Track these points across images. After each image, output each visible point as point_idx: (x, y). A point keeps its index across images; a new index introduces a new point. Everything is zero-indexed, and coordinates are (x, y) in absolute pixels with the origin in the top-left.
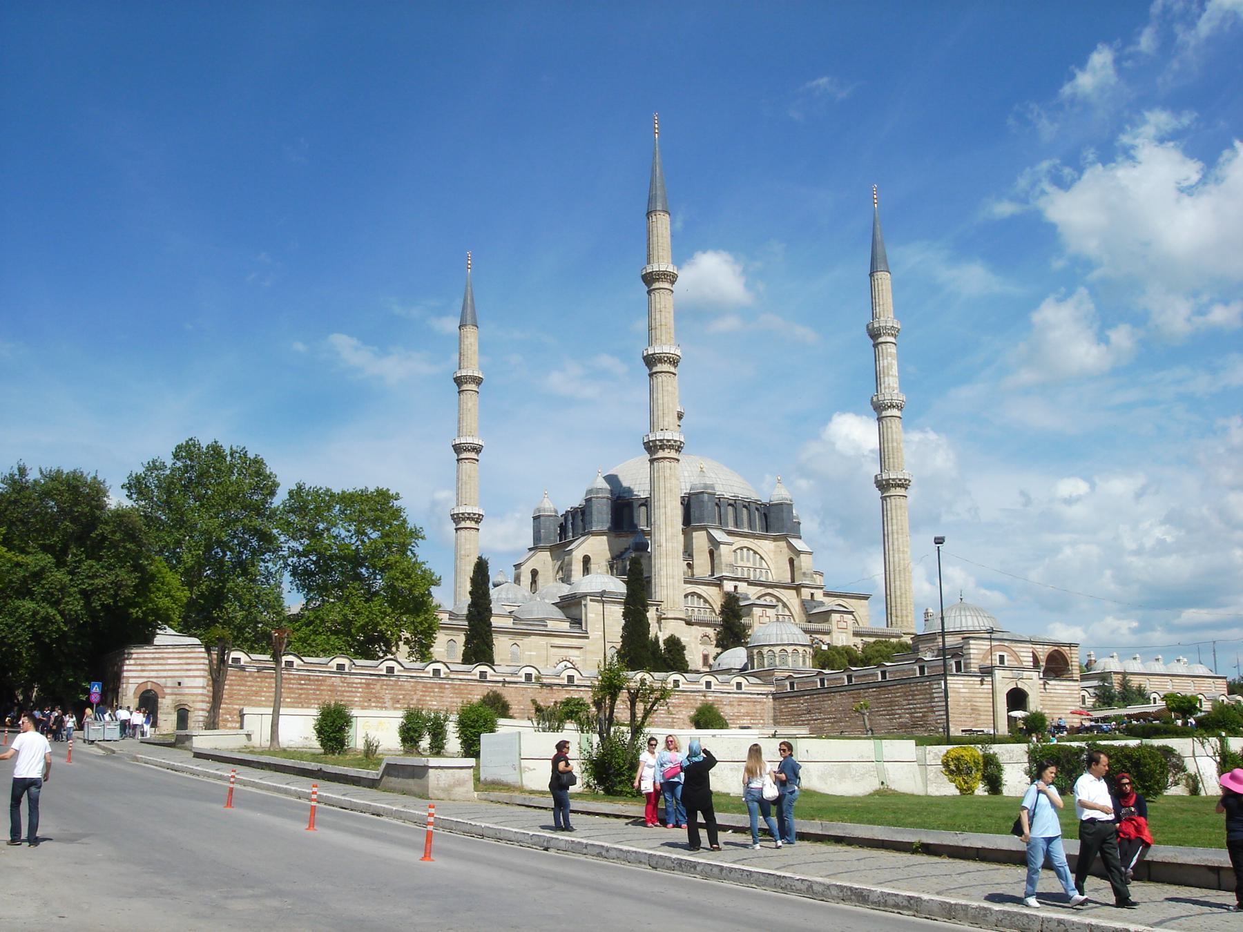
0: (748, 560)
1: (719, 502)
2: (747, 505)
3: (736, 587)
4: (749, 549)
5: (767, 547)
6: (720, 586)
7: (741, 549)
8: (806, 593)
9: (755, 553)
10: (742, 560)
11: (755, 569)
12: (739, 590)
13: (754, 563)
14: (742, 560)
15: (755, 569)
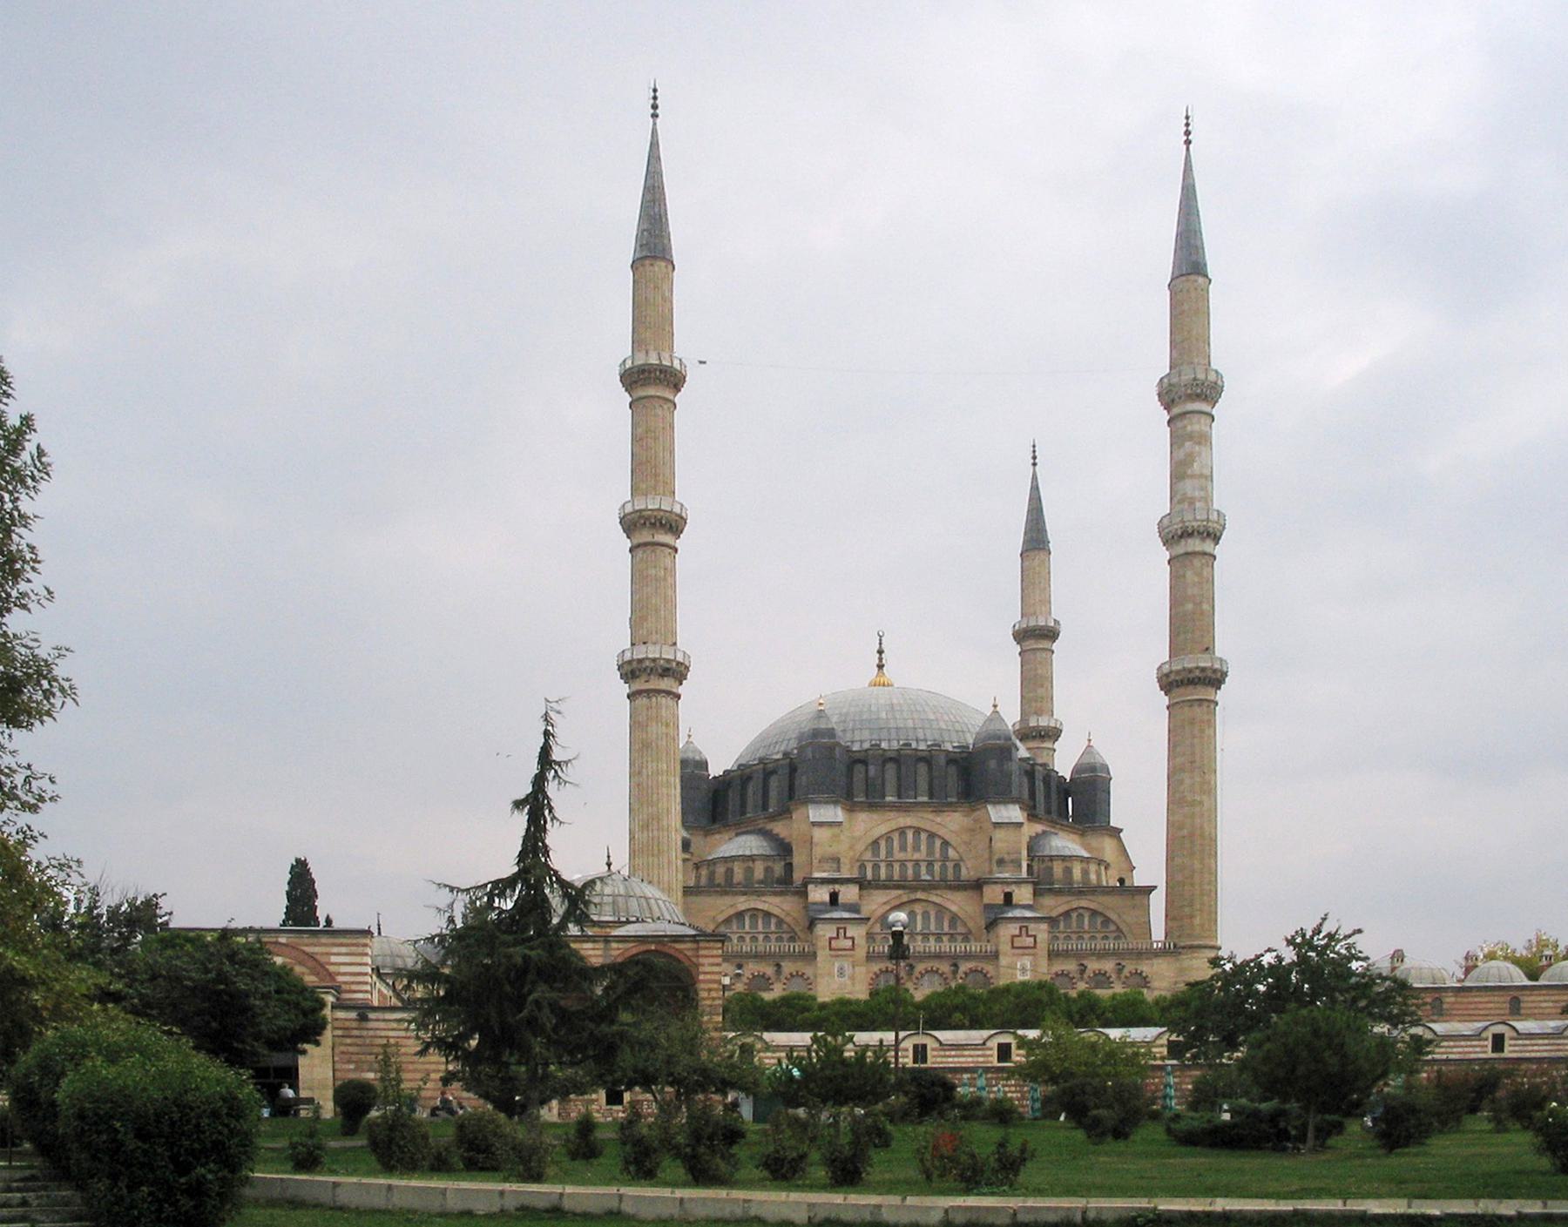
0: (916, 848)
1: (858, 760)
2: (927, 759)
3: (834, 897)
4: (917, 831)
5: (952, 823)
6: (803, 893)
7: (902, 831)
8: (994, 895)
9: (932, 835)
10: (903, 848)
11: (930, 864)
12: (841, 899)
13: (930, 851)
14: (903, 848)
15: (930, 864)
